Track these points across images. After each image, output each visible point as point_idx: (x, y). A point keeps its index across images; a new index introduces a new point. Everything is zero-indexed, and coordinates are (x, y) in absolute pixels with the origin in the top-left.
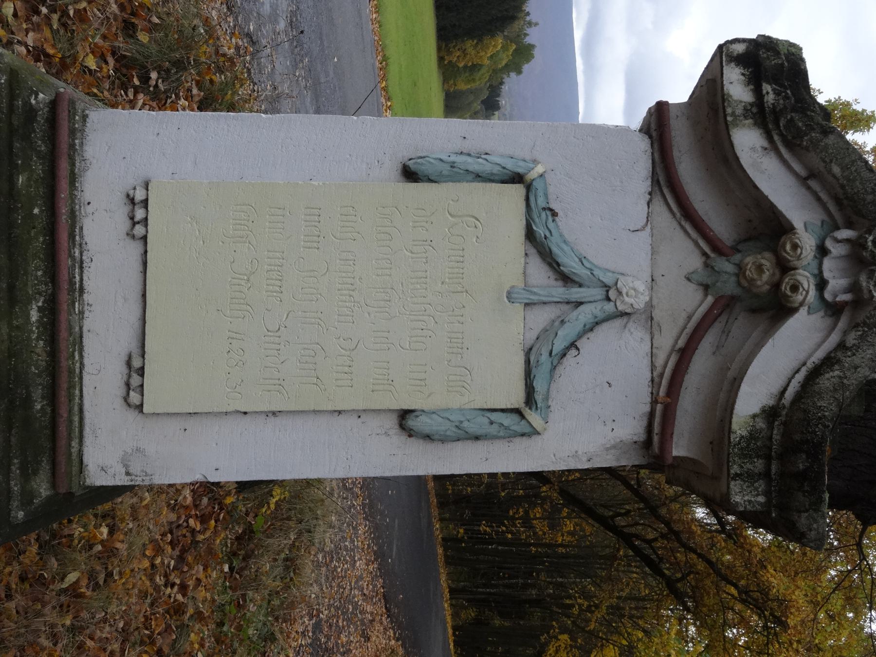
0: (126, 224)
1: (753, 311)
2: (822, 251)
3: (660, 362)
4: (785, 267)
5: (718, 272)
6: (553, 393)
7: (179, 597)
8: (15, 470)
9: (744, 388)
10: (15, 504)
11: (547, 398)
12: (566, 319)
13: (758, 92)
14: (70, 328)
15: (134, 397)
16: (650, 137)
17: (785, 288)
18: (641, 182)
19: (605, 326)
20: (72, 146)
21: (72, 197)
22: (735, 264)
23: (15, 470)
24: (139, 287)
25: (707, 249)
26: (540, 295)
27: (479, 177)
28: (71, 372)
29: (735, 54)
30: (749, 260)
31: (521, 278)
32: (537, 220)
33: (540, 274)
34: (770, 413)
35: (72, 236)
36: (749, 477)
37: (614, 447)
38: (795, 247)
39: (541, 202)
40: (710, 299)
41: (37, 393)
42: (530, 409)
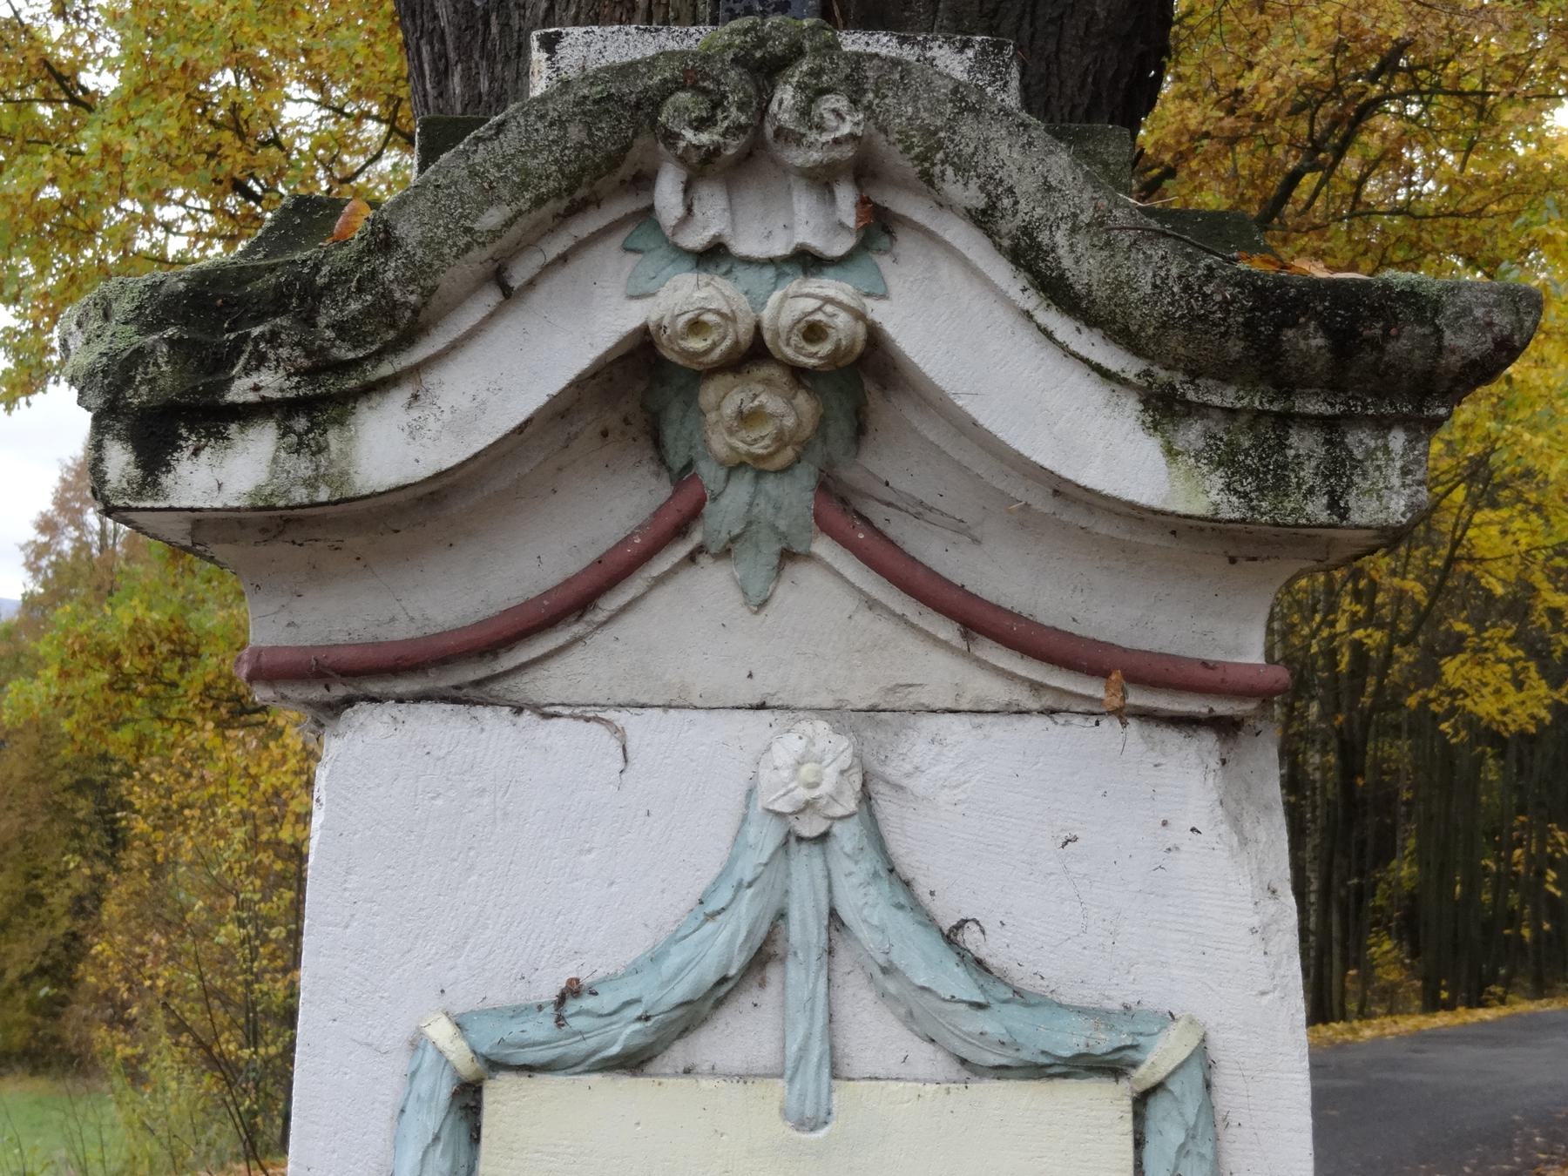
1: (860, 431)
2: (714, 255)
3: (998, 692)
5: (750, 523)
6: (1086, 996)
9: (1091, 477)
11: (1098, 1015)
12: (881, 960)
13: (247, 414)
16: (349, 702)
17: (812, 356)
18: (484, 736)
19: (898, 846)
22: (728, 479)
25: (681, 550)
26: (808, 1036)
29: (136, 473)
30: (719, 443)
31: (758, 1088)
32: (592, 1043)
37: (1236, 821)
38: (696, 326)
39: (540, 1027)
40: (824, 547)
42: (1135, 1065)
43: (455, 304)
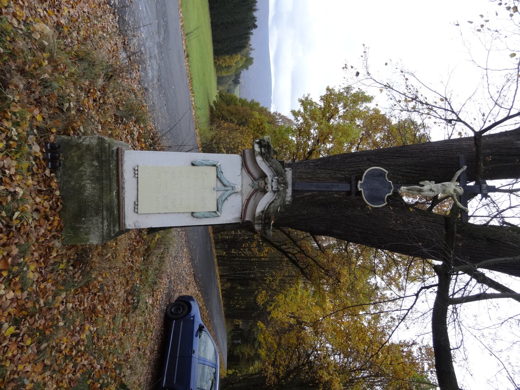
0: (134, 174)
1: (262, 192)
2: (272, 181)
3: (243, 202)
4: (266, 184)
6: (222, 208)
7: (131, 264)
8: (112, 225)
10: (112, 232)
11: (221, 209)
13: (261, 149)
14: (122, 196)
15: (136, 210)
17: (266, 188)
19: (232, 196)
20: (122, 158)
21: (122, 169)
23: (112, 225)
24: (137, 187)
27: (207, 165)
28: (123, 205)
30: (260, 182)
33: (219, 184)
34: (263, 212)
35: (122, 177)
36: (258, 224)
38: (268, 180)
39: (220, 170)
40: (253, 189)
41: (115, 210)
43: (269, 163)
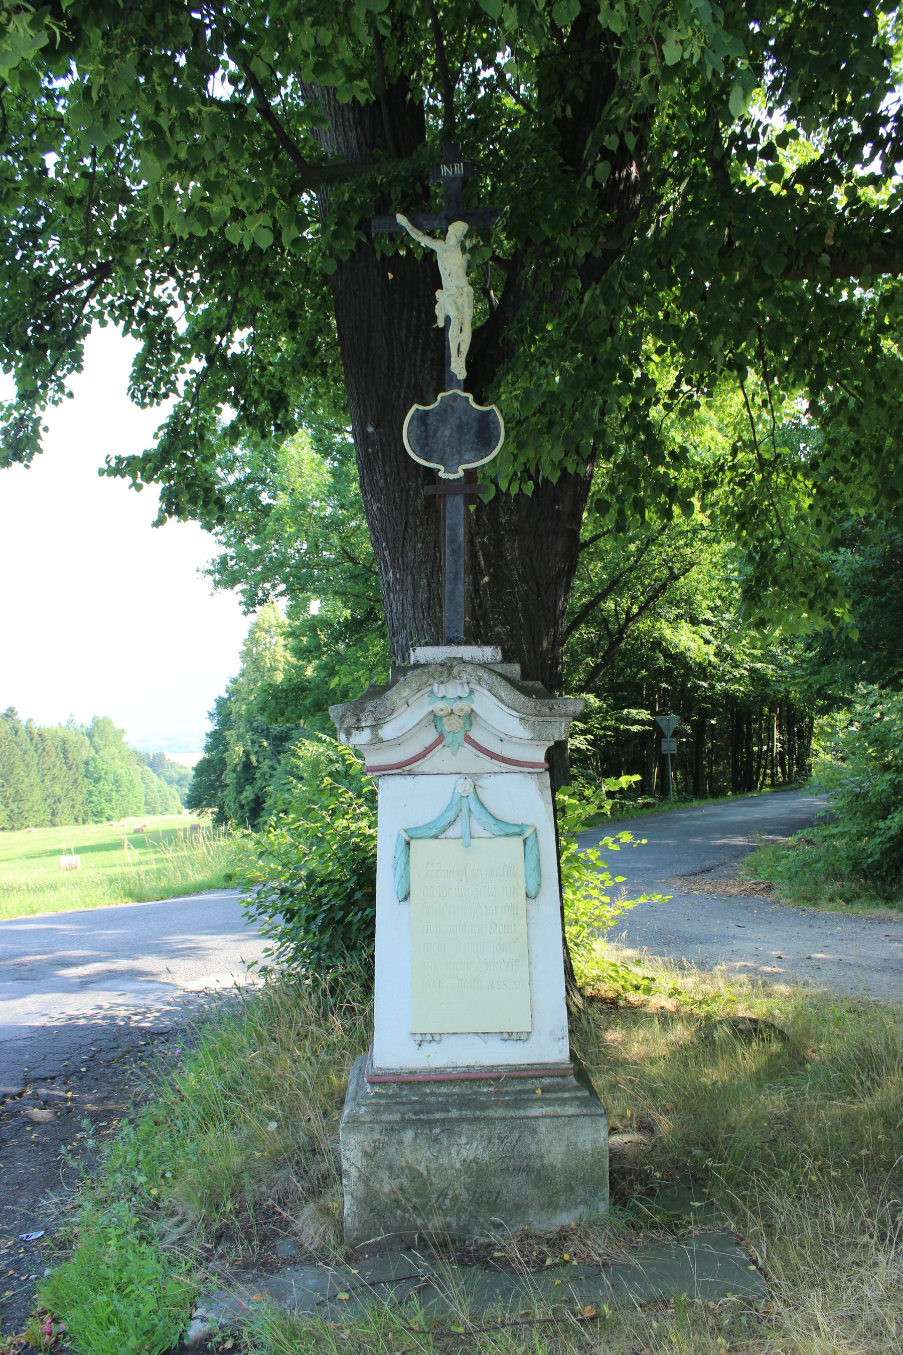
15: (524, 1036)
20: (393, 1074)
27: (408, 862)
33: (453, 831)
37: (541, 790)
40: (466, 745)
